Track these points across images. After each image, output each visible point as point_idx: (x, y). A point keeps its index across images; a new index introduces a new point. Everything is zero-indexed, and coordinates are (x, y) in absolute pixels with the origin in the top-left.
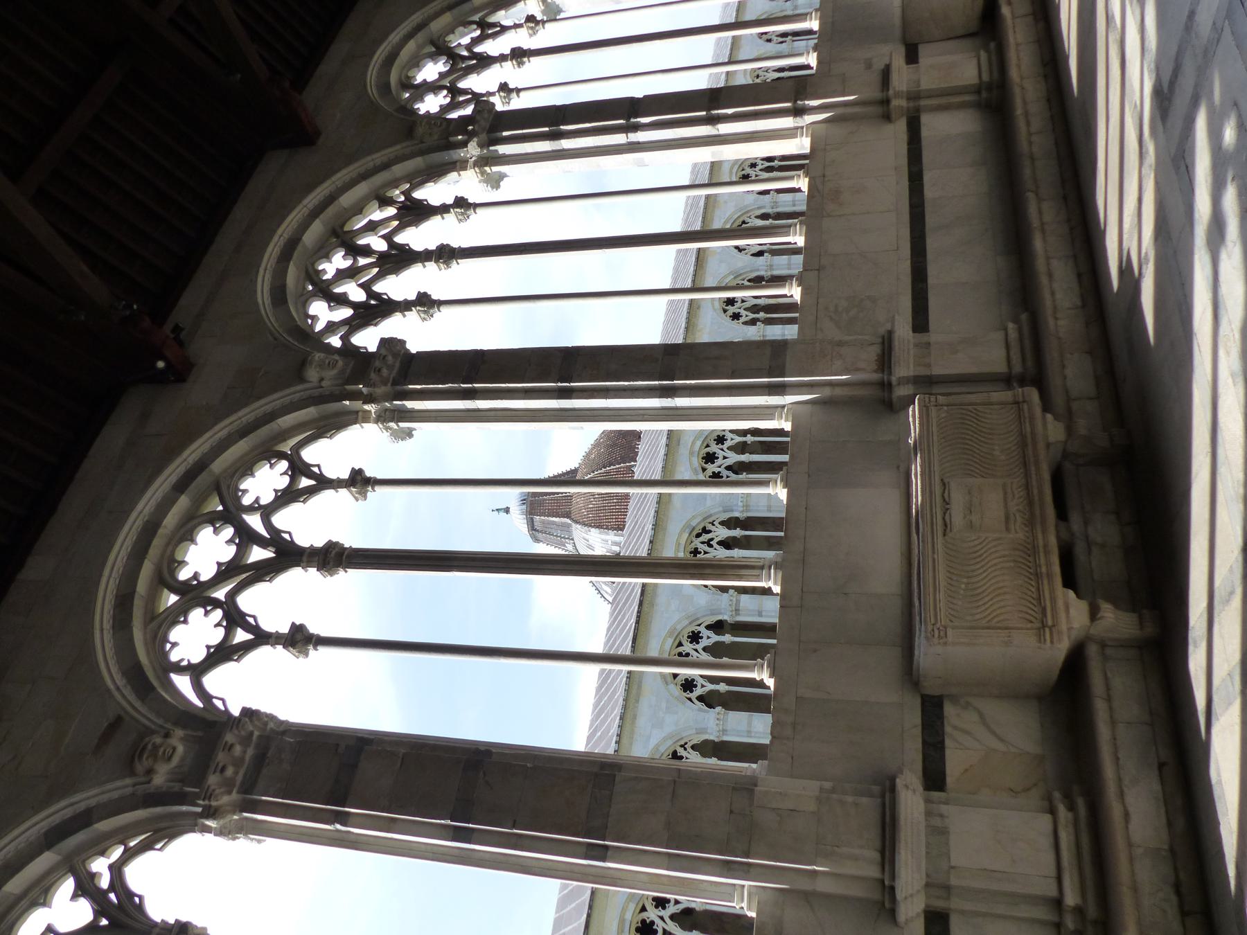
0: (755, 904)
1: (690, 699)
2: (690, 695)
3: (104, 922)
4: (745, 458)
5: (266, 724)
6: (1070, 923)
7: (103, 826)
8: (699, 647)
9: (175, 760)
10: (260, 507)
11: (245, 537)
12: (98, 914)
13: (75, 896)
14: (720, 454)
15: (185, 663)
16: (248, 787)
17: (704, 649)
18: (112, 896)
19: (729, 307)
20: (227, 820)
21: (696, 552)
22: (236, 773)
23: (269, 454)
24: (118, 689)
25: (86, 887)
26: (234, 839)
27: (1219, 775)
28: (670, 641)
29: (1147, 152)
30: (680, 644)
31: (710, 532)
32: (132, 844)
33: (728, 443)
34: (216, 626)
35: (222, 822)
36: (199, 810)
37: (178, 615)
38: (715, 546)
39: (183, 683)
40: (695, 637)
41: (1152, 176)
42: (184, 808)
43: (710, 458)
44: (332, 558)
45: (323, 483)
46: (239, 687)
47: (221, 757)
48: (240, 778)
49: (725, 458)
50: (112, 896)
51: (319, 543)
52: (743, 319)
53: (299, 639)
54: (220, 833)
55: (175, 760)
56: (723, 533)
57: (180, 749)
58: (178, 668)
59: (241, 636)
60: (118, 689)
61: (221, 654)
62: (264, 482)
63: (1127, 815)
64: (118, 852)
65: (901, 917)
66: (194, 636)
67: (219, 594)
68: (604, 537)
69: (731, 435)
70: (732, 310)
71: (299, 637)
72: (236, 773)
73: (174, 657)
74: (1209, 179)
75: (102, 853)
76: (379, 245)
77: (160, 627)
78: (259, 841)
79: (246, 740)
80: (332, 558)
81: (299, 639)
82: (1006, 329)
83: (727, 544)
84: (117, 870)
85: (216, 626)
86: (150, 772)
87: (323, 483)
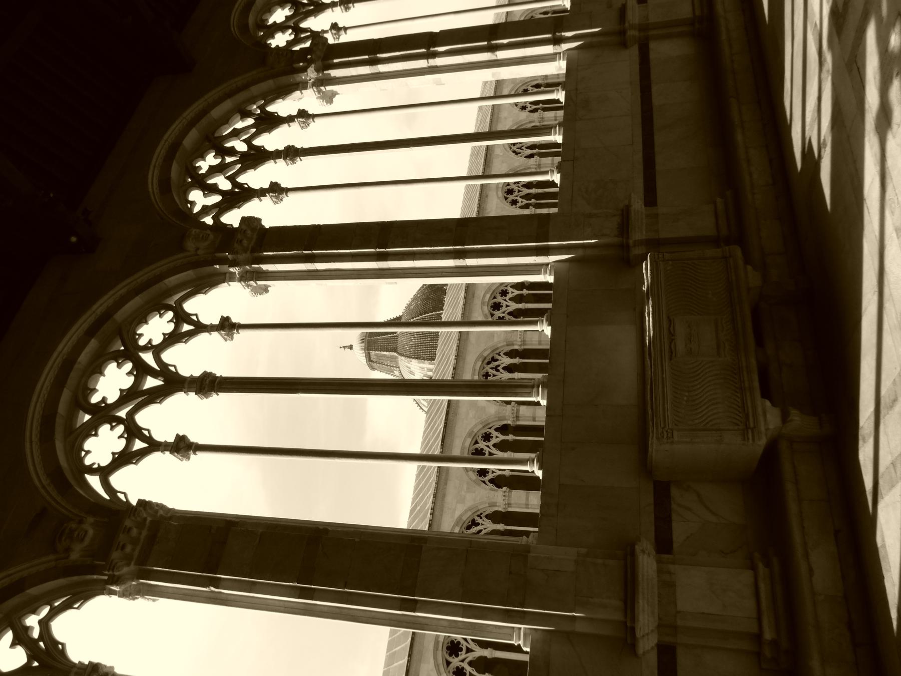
0: (529, 643)
1: (484, 482)
2: (484, 479)
3: (36, 664)
4: (521, 306)
5: (157, 512)
6: (767, 652)
7: (33, 591)
8: (490, 444)
9: (87, 541)
10: (153, 347)
11: (141, 371)
12: (31, 658)
13: (13, 645)
14: (504, 303)
15: (96, 466)
16: (143, 560)
17: (495, 445)
18: (41, 644)
19: (509, 196)
20: (127, 585)
21: (487, 375)
22: (133, 550)
23: (160, 307)
24: (44, 487)
25: (22, 638)
26: (134, 599)
27: (883, 540)
28: (469, 440)
29: (825, 60)
30: (476, 442)
32: (56, 604)
33: (510, 296)
34: (119, 437)
35: (123, 587)
36: (106, 578)
37: (91, 430)
38: (501, 370)
39: (94, 481)
40: (487, 437)
41: (830, 78)
42: (89, 577)
43: (497, 306)
44: (207, 384)
45: (200, 328)
46: (136, 484)
47: (122, 538)
48: (136, 553)
49: (507, 306)
50: (41, 644)
51: (197, 374)
52: (519, 205)
53: (182, 446)
54: (123, 595)
55: (87, 541)
56: (507, 361)
57: (91, 532)
58: (91, 470)
59: (139, 445)
60: (44, 487)
61: (123, 459)
62: (155, 328)
63: (811, 571)
64: (45, 611)
65: (640, 651)
66: (102, 446)
67: (122, 413)
69: (510, 290)
70: (511, 197)
71: (182, 445)
72: (133, 550)
73: (88, 461)
74: (878, 77)
75: (34, 611)
76: (240, 146)
77: (76, 439)
78: (154, 600)
79: (141, 525)
80: (207, 384)
81: (182, 446)
83: (510, 369)
84: (45, 624)
85: (119, 437)
86: (68, 550)
87: (200, 328)
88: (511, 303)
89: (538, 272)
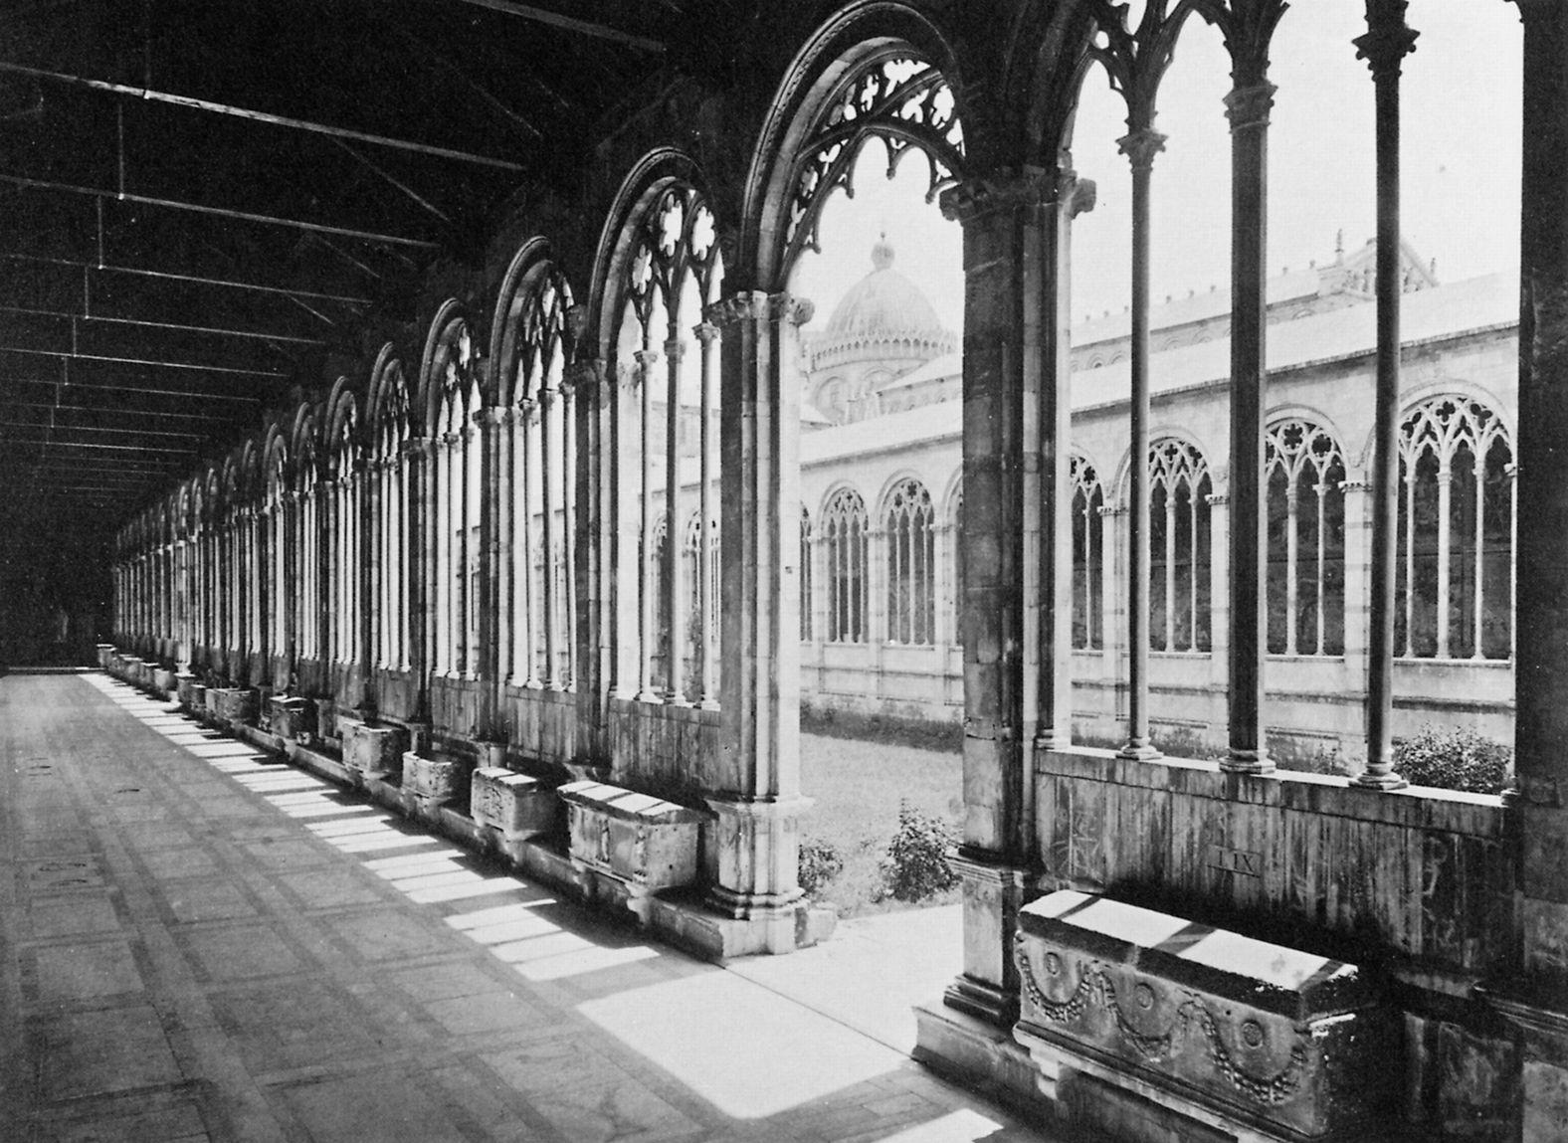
2: (1310, 451)
14: (1300, 449)
31: (1195, 464)
38: (1423, 443)
68: (1401, 289)
69: (1328, 457)
82: (1406, 868)
88: (1299, 466)
89: (916, 547)
